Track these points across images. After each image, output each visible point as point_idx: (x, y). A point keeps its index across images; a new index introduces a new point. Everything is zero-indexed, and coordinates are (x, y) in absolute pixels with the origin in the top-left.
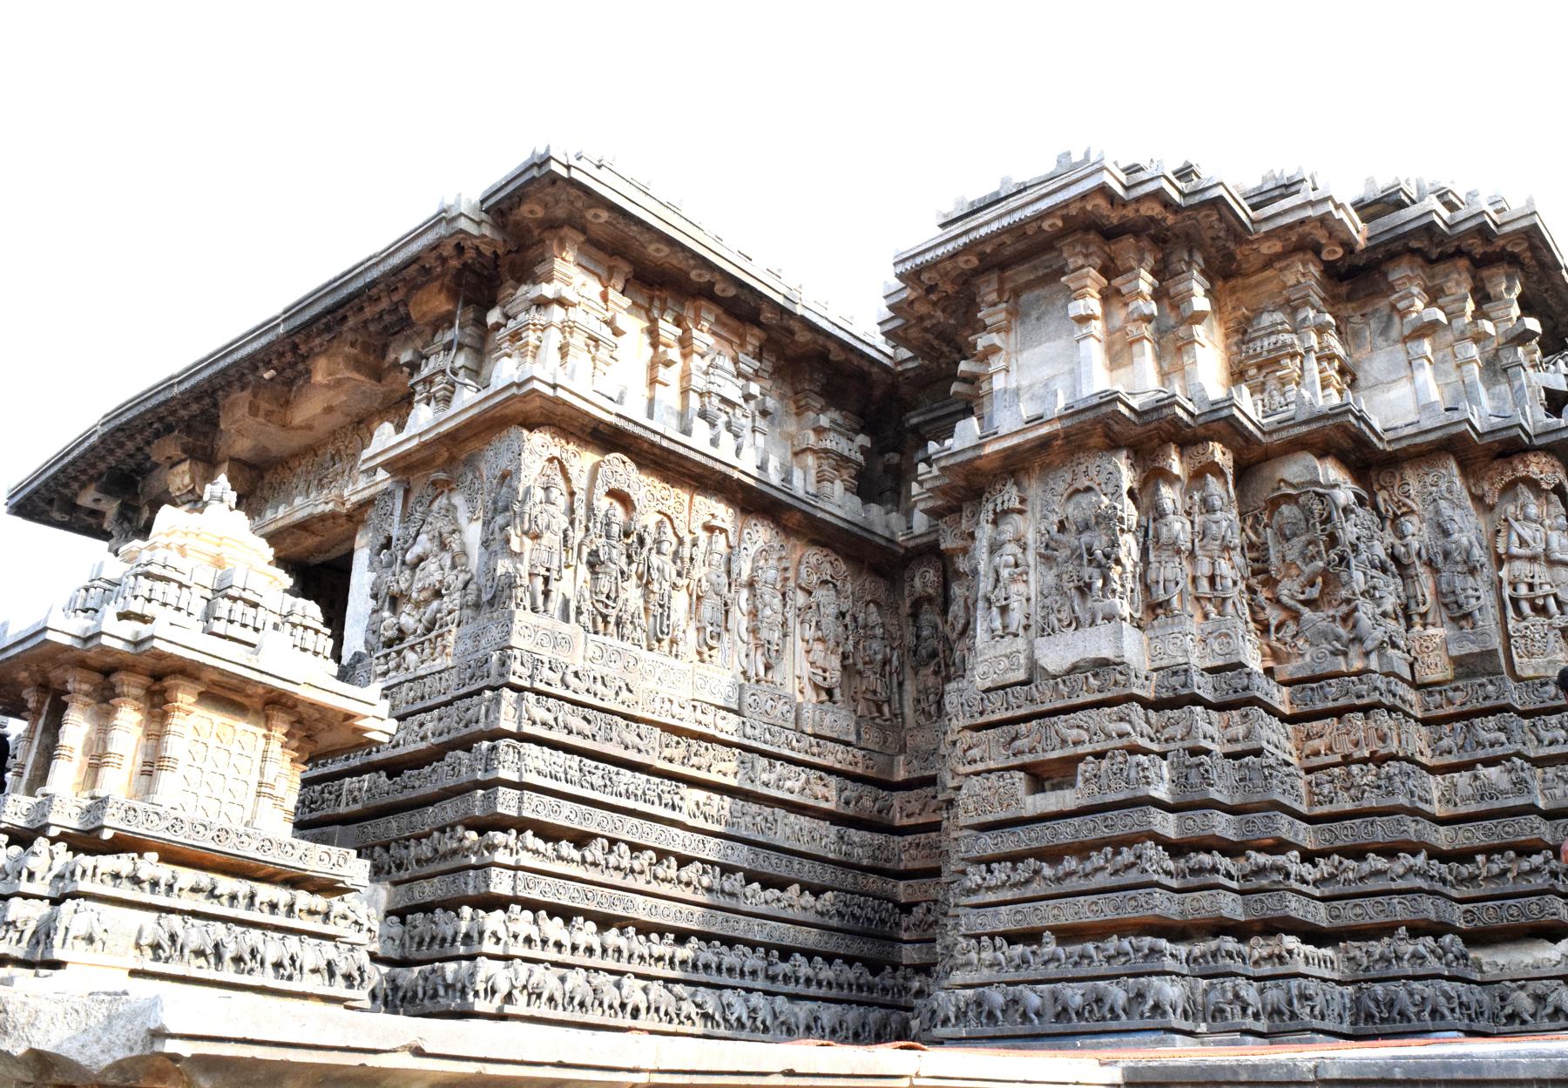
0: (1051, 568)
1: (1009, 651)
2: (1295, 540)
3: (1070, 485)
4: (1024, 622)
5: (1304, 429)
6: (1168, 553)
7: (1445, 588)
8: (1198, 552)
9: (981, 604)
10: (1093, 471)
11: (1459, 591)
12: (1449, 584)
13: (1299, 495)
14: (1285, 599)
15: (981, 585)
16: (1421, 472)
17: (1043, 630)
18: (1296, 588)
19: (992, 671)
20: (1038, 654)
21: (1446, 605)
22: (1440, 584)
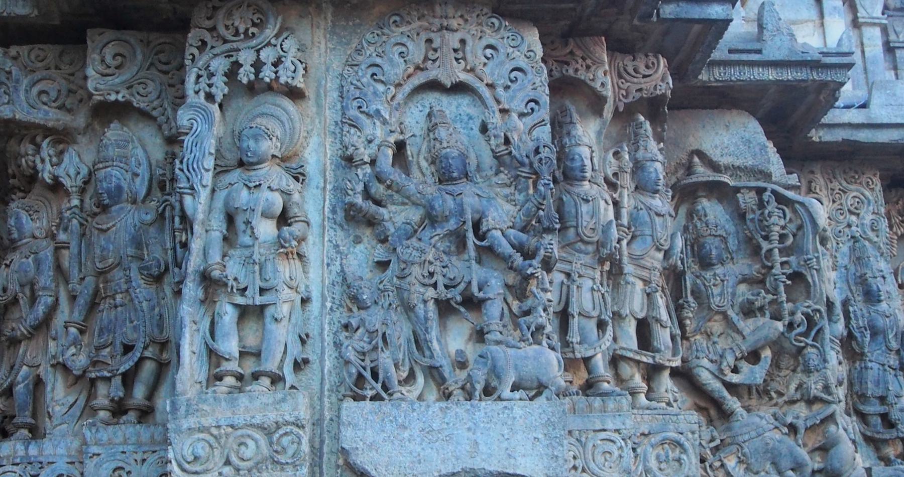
0: (358, 240)
1: (272, 417)
2: (719, 270)
3: (418, 68)
4: (295, 351)
5: (771, 75)
6: (587, 259)
7: (871, 389)
8: (628, 268)
9: (192, 290)
10: (475, 52)
11: (891, 399)
12: (877, 383)
13: (737, 190)
14: (706, 377)
15: (196, 245)
16: (836, 185)
17: (360, 379)
18: (730, 359)
19: (219, 459)
20: (348, 437)
21: (863, 417)
22: (862, 381)
